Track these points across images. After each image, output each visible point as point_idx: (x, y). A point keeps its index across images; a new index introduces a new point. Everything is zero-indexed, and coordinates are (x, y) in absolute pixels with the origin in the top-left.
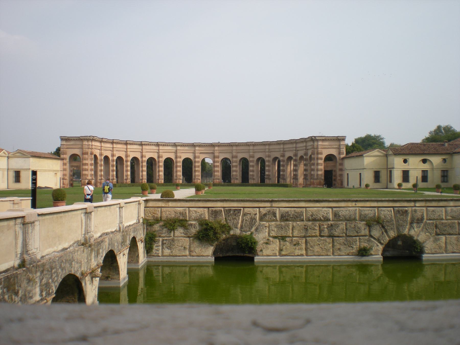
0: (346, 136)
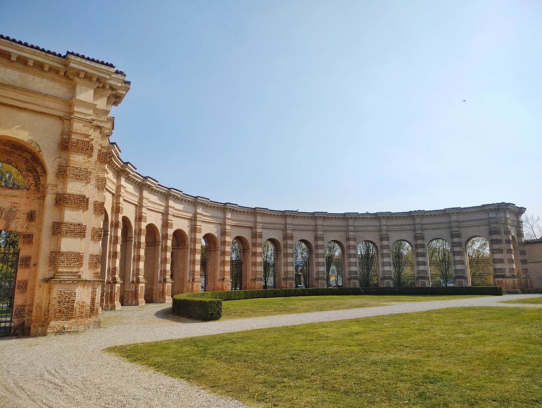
0: (526, 209)
